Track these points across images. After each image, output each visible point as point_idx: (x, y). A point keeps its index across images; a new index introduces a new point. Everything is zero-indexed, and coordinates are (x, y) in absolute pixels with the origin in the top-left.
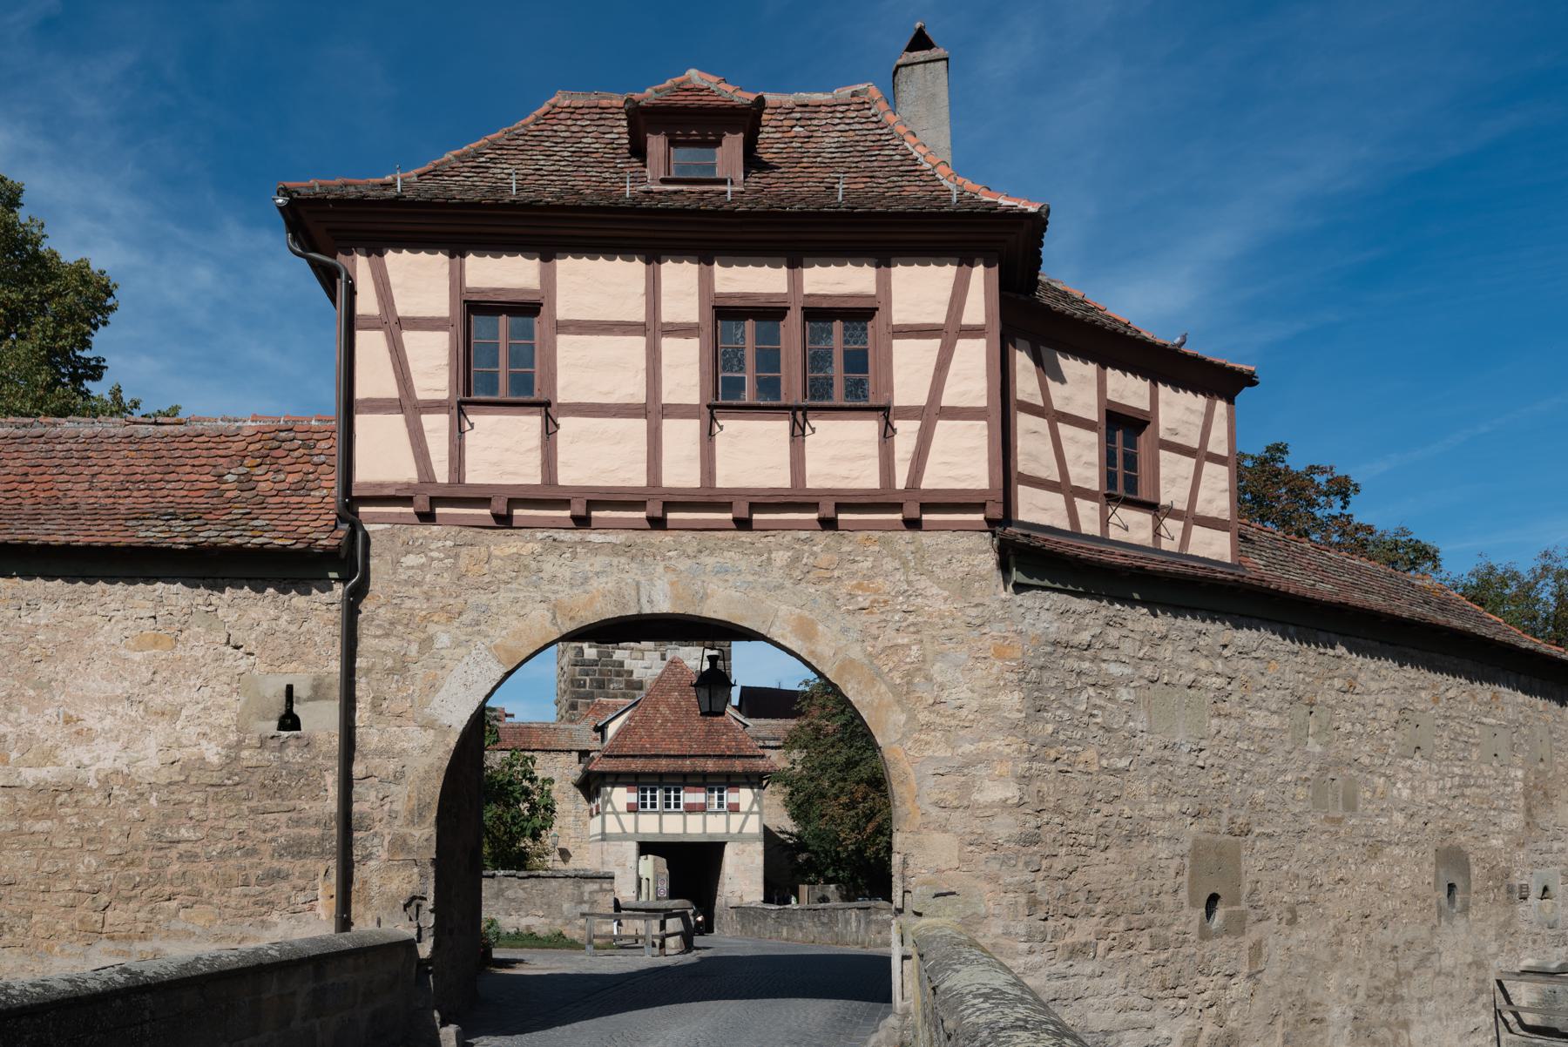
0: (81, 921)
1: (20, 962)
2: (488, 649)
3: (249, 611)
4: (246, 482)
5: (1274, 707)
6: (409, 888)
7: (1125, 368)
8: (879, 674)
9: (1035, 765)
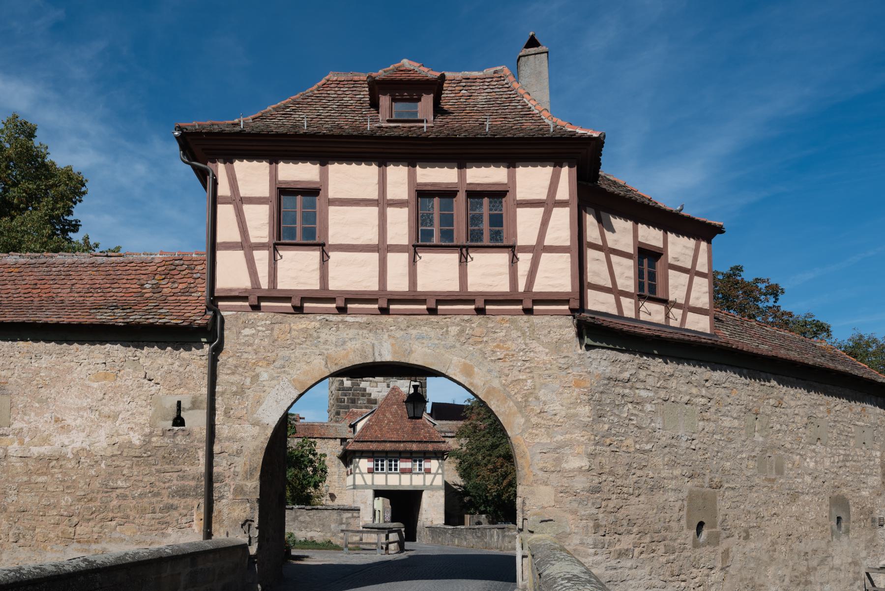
0: (62, 532)
1: (28, 555)
2: (289, 381)
3: (157, 359)
4: (156, 288)
5: (735, 415)
6: (245, 515)
7: (649, 223)
8: (509, 396)
9: (598, 447)
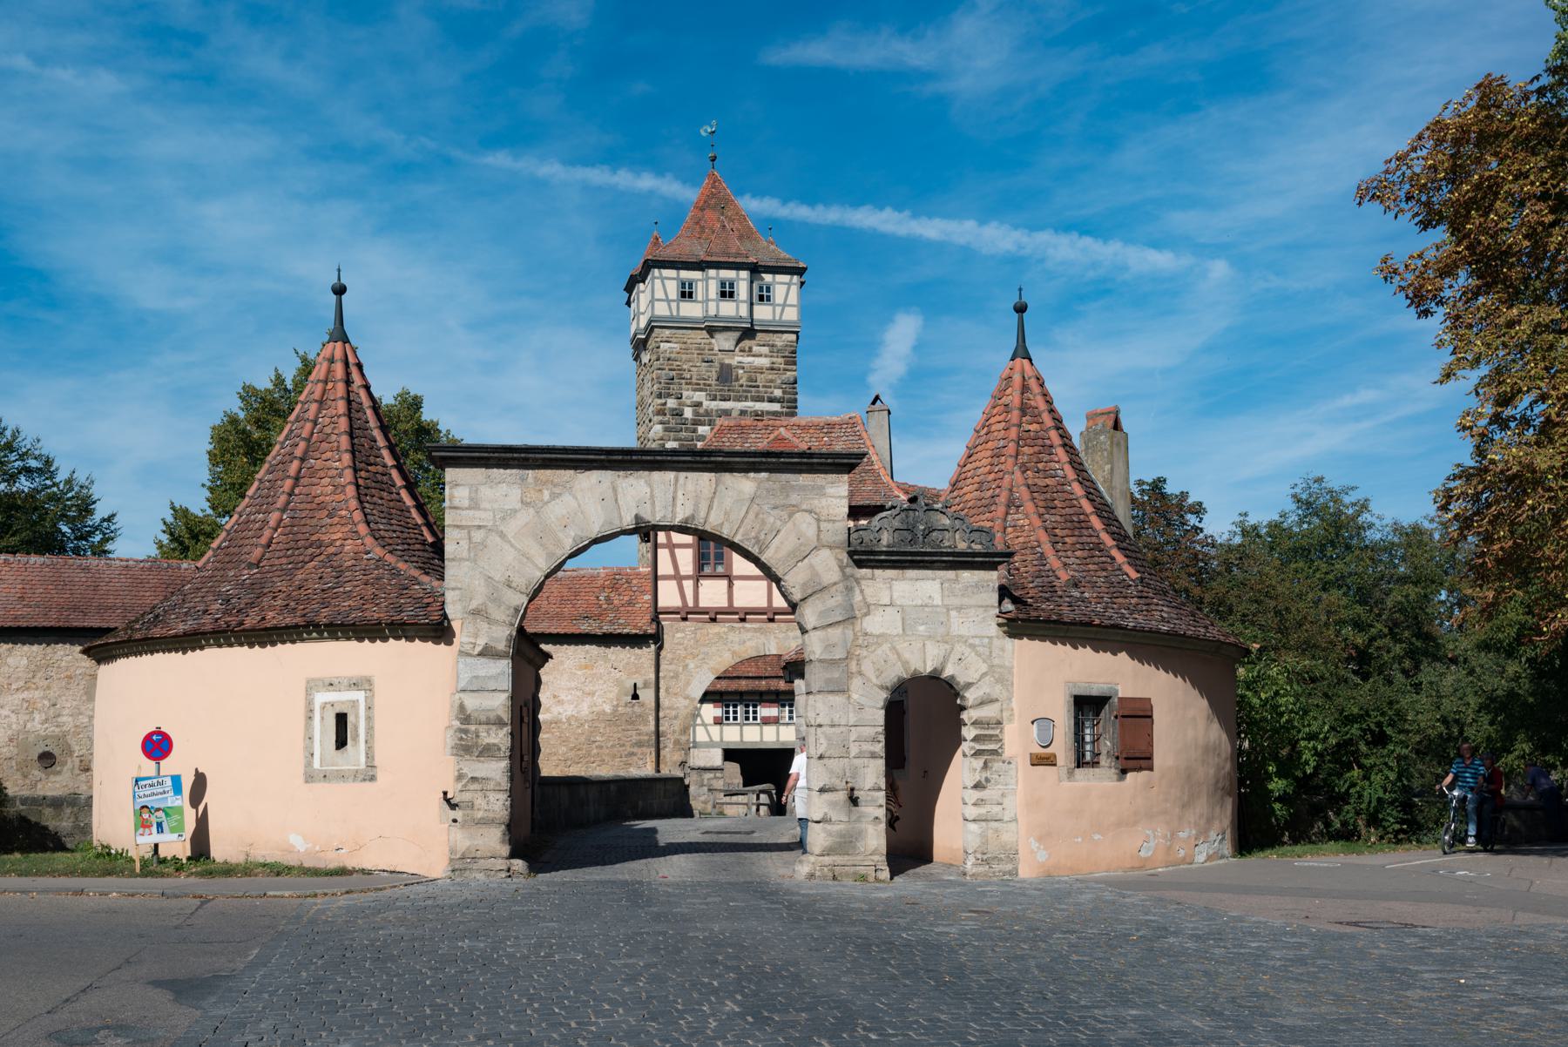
3: (618, 654)
